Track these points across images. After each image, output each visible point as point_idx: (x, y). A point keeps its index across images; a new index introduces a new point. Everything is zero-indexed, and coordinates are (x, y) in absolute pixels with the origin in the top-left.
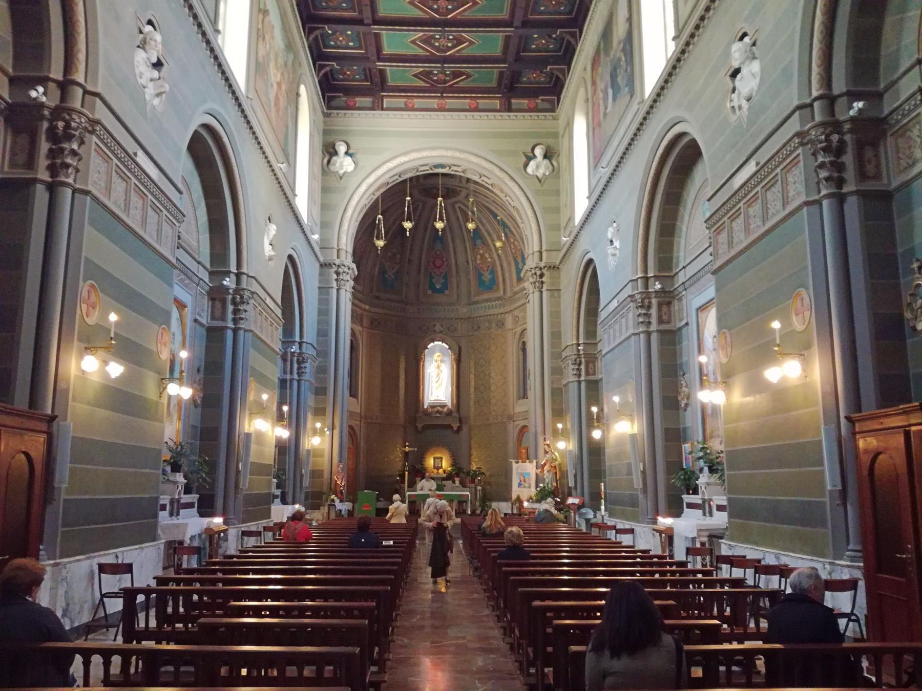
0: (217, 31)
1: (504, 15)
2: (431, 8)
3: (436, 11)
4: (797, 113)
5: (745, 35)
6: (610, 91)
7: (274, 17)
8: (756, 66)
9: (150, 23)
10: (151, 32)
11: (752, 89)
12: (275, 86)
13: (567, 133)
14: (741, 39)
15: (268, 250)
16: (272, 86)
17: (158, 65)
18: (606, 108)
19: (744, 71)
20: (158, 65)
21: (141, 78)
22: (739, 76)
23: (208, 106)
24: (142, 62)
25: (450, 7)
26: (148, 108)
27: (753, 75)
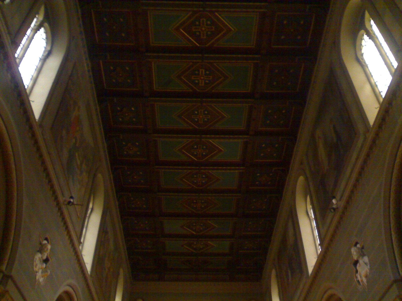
0: (80, 243)
1: (242, 127)
2: (192, 229)
3: (195, 156)
4: (395, 286)
5: (357, 243)
6: (289, 272)
7: (111, 235)
8: (366, 259)
9: (46, 239)
10: (46, 244)
11: (367, 271)
12: (107, 269)
13: (290, 224)
14: (356, 245)
15: (41, 280)
16: (105, 270)
17: (46, 261)
18: (288, 279)
19: (361, 261)
20: (46, 261)
21: (36, 267)
22: (358, 265)
23: (71, 281)
24: (38, 259)
25: (203, 206)
26: (37, 283)
27: (366, 263)
